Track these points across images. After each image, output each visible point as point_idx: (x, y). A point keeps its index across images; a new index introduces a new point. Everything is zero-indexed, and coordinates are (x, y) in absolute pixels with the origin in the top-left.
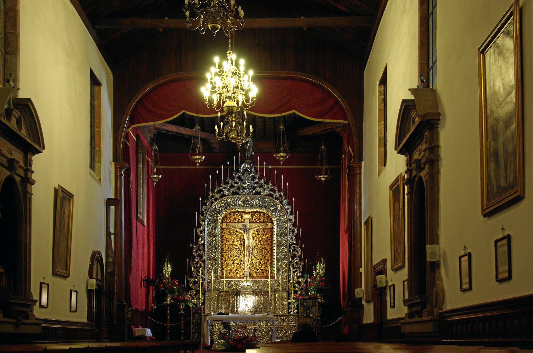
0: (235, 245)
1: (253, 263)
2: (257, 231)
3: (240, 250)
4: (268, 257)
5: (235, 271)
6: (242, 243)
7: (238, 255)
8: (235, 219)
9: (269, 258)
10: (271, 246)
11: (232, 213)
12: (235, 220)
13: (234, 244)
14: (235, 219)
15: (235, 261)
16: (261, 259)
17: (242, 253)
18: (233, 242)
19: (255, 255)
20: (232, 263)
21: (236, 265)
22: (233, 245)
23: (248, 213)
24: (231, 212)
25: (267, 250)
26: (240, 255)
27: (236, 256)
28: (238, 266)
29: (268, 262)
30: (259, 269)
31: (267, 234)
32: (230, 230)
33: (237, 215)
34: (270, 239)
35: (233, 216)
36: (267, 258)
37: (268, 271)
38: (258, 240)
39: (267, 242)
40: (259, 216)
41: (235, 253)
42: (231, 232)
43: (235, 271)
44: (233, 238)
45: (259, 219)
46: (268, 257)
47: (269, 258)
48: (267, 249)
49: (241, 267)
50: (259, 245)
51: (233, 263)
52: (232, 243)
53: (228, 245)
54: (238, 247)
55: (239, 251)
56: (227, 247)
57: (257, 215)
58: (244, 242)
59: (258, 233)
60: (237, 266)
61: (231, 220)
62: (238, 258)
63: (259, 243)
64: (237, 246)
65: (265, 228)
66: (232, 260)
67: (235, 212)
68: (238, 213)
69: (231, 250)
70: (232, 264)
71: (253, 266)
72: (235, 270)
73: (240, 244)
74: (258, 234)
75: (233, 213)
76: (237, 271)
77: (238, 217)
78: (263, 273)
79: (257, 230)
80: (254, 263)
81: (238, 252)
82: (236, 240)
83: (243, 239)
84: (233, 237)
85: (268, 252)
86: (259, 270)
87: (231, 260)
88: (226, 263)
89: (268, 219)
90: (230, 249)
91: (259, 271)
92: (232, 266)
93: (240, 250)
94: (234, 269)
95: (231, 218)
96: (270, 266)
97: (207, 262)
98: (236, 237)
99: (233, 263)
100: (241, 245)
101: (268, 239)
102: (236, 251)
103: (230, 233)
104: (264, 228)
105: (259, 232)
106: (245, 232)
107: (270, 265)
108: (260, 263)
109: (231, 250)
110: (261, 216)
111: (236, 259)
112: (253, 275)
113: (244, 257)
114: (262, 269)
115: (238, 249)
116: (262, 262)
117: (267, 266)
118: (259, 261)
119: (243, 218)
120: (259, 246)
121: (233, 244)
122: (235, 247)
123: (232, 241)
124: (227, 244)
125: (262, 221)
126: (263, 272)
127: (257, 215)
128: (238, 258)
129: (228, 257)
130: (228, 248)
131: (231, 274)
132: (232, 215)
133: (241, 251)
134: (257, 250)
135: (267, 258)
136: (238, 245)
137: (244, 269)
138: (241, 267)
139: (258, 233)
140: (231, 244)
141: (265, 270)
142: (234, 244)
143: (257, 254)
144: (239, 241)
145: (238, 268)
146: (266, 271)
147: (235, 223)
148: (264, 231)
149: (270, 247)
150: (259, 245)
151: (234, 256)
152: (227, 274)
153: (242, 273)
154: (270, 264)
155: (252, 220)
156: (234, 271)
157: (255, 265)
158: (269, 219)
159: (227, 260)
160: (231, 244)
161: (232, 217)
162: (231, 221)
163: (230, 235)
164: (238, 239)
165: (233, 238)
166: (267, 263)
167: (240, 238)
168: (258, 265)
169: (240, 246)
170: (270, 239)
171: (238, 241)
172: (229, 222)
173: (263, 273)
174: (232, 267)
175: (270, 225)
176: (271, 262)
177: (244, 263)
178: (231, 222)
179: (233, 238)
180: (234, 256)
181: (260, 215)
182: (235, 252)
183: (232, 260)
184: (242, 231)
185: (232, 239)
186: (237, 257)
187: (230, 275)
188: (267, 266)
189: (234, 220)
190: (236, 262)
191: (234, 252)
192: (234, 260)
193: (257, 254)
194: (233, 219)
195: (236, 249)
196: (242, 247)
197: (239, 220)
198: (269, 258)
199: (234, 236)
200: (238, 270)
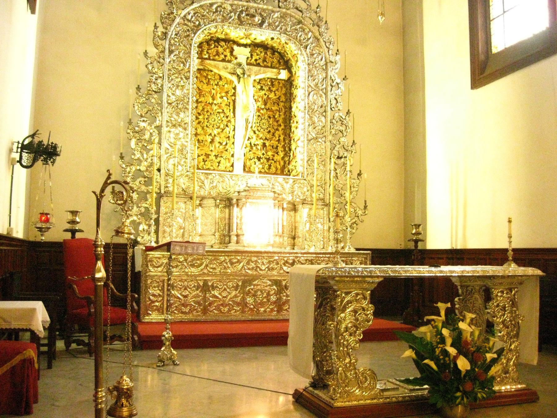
0: (216, 105)
1: (251, 143)
2: (259, 83)
3: (227, 117)
4: (279, 136)
5: (216, 158)
6: (229, 103)
7: (222, 126)
8: (218, 54)
9: (280, 138)
10: (284, 115)
11: (213, 42)
12: (219, 56)
13: (215, 102)
14: (218, 54)
15: (216, 138)
16: (266, 139)
17: (229, 121)
18: (213, 99)
19: (255, 129)
20: (209, 140)
21: (218, 145)
22: (213, 106)
23: (245, 46)
24: (211, 40)
25: (277, 121)
26: (227, 126)
27: (218, 128)
28: (221, 147)
29: (279, 145)
30: (262, 156)
31: (277, 90)
32: (207, 75)
33: (221, 46)
34: (282, 102)
35: (214, 47)
36: (277, 136)
37: (278, 163)
38: (260, 99)
39: (278, 105)
40: (263, 54)
41: (216, 121)
42: (209, 79)
43: (216, 158)
44: (212, 90)
45: (264, 60)
46: (279, 136)
47: (280, 138)
48: (277, 119)
49: (226, 150)
50: (263, 109)
51: (212, 141)
52: (211, 100)
53: (203, 104)
54: (223, 110)
55: (223, 119)
56: (201, 108)
57: (261, 52)
58: (234, 101)
59: (262, 87)
60: (219, 147)
61: (211, 55)
62: (222, 132)
63: (263, 107)
64: (220, 107)
65: (277, 79)
66: (210, 134)
67: (218, 40)
68: (224, 44)
69: (209, 114)
70: (211, 142)
71: (250, 151)
72: (216, 156)
73: (226, 105)
74: (262, 89)
75: (215, 42)
76: (219, 159)
77: (225, 50)
78: (270, 166)
79: (260, 80)
80: (253, 145)
81: (222, 121)
82: (219, 95)
83: (232, 96)
84: (213, 89)
85: (280, 125)
86: (262, 158)
87: (209, 135)
88: (198, 140)
89: (280, 63)
90: (207, 112)
91: (262, 161)
92: (209, 147)
93: (227, 117)
94: (214, 154)
95: (210, 51)
96: (283, 153)
97: (165, 130)
98: (220, 89)
99: (212, 141)
100: (229, 107)
101: (279, 99)
102: (219, 118)
103: (207, 80)
104: (274, 79)
105: (264, 84)
106: (241, 79)
107: (284, 151)
108: (264, 145)
109: (209, 114)
110: (267, 55)
111: (219, 134)
112: (250, 168)
113: (234, 130)
114: (268, 157)
115: (222, 113)
116: (267, 144)
117: (277, 153)
118: (262, 141)
119: (234, 53)
120: (262, 111)
121: (212, 103)
122: (216, 110)
123: (212, 97)
124: (201, 102)
125: (269, 65)
126: (269, 163)
127: (261, 52)
128: (222, 132)
129: (203, 128)
130: (203, 109)
131: (206, 163)
132: (213, 45)
133: (229, 119)
134: (260, 119)
135: (277, 136)
136: (223, 105)
137: (233, 156)
138: (226, 150)
139: (262, 87)
140: (209, 103)
141: (273, 160)
142: (215, 102)
143: (259, 128)
144: (225, 98)
145: (222, 152)
146: (275, 162)
147: (218, 61)
148: (272, 85)
149: (283, 116)
150: (263, 109)
151: (213, 127)
152: (199, 163)
153: (229, 162)
154: (282, 149)
155: (251, 60)
156: (214, 158)
157: (254, 148)
158: (282, 63)
159: (199, 135)
160: (209, 103)
161: (212, 50)
162: (209, 56)
163: (208, 83)
164: (223, 94)
165: (212, 90)
166: (277, 146)
167: (227, 93)
168: (261, 150)
169: (227, 109)
170: (282, 102)
171: (222, 97)
172: (206, 59)
173: (270, 166)
174: (210, 150)
175: (284, 75)
176: (284, 145)
177: (233, 143)
178: (209, 59)
179: (213, 91)
180: (213, 127)
181: (266, 53)
182: (217, 120)
183: (210, 134)
184: (234, 78)
185: (210, 92)
186: (219, 130)
187: (205, 164)
188: (277, 153)
189: (215, 56)
190: (217, 139)
191: (215, 120)
192: (213, 135)
193: (259, 128)
194: (215, 53)
195: (219, 113)
196: (230, 110)
197: (226, 56)
198: (282, 138)
199: (215, 87)
200: (222, 157)
